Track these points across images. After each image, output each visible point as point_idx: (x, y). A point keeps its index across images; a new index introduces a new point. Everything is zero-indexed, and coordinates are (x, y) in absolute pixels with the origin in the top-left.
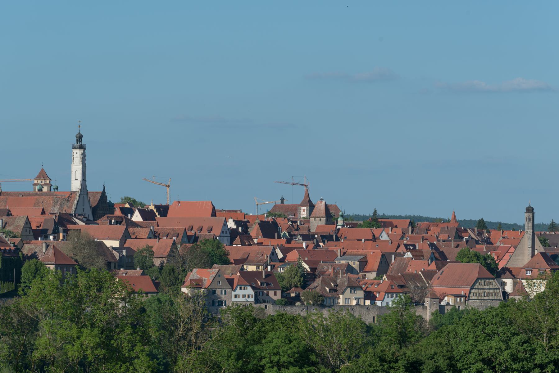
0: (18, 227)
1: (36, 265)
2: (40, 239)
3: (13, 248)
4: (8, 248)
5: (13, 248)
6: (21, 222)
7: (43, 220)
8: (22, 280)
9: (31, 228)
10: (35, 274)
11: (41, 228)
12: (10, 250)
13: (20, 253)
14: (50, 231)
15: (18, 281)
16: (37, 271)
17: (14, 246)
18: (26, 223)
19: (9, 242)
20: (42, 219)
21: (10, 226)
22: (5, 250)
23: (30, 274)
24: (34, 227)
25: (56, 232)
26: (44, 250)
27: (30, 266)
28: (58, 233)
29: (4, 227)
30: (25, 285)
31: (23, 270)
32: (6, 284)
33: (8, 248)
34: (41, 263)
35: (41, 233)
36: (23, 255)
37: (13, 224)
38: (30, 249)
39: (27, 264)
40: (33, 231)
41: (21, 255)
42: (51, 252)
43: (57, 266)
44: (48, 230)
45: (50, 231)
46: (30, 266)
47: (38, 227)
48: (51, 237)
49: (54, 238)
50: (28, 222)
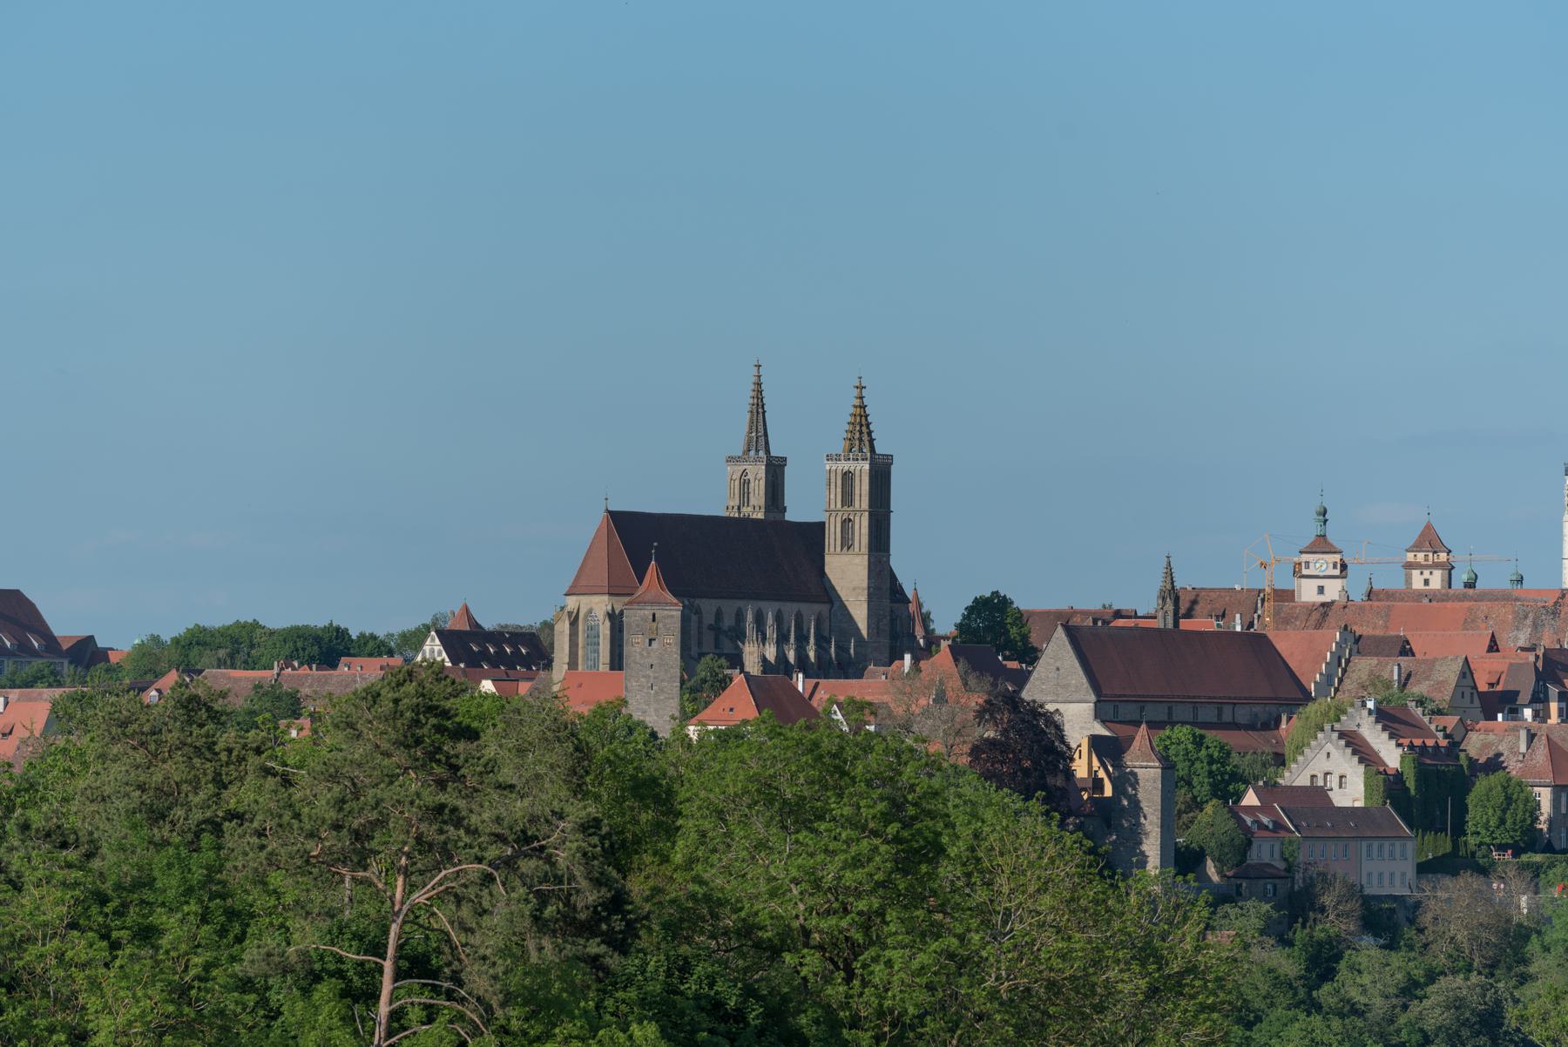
0: (1441, 683)
1: (1505, 788)
2: (1500, 716)
3: (1444, 743)
4: (1430, 743)
5: (1444, 743)
6: (1449, 673)
7: (1504, 668)
8: (1470, 827)
9: (1475, 687)
10: (1504, 811)
11: (1499, 688)
12: (1437, 746)
13: (1462, 755)
14: (1525, 697)
15: (1459, 830)
16: (1509, 804)
17: (1446, 736)
18: (1463, 675)
19: (1433, 727)
20: (1497, 663)
21: (1419, 682)
22: (1424, 746)
23: (1490, 812)
24: (1483, 687)
25: (1539, 699)
26: (1523, 748)
27: (1491, 790)
28: (1546, 701)
29: (1405, 685)
30: (1478, 839)
31: (1471, 799)
32: (1429, 837)
33: (1430, 743)
34: (1520, 784)
35: (1499, 702)
36: (1470, 759)
37: (1427, 678)
38: (1486, 746)
39: (1482, 784)
40: (1481, 694)
41: (1464, 762)
42: (1541, 754)
43: (1558, 790)
44: (1517, 693)
45: (1525, 697)
46: (1491, 790)
47: (1491, 685)
48: (1528, 713)
49: (1536, 715)
50: (1467, 672)
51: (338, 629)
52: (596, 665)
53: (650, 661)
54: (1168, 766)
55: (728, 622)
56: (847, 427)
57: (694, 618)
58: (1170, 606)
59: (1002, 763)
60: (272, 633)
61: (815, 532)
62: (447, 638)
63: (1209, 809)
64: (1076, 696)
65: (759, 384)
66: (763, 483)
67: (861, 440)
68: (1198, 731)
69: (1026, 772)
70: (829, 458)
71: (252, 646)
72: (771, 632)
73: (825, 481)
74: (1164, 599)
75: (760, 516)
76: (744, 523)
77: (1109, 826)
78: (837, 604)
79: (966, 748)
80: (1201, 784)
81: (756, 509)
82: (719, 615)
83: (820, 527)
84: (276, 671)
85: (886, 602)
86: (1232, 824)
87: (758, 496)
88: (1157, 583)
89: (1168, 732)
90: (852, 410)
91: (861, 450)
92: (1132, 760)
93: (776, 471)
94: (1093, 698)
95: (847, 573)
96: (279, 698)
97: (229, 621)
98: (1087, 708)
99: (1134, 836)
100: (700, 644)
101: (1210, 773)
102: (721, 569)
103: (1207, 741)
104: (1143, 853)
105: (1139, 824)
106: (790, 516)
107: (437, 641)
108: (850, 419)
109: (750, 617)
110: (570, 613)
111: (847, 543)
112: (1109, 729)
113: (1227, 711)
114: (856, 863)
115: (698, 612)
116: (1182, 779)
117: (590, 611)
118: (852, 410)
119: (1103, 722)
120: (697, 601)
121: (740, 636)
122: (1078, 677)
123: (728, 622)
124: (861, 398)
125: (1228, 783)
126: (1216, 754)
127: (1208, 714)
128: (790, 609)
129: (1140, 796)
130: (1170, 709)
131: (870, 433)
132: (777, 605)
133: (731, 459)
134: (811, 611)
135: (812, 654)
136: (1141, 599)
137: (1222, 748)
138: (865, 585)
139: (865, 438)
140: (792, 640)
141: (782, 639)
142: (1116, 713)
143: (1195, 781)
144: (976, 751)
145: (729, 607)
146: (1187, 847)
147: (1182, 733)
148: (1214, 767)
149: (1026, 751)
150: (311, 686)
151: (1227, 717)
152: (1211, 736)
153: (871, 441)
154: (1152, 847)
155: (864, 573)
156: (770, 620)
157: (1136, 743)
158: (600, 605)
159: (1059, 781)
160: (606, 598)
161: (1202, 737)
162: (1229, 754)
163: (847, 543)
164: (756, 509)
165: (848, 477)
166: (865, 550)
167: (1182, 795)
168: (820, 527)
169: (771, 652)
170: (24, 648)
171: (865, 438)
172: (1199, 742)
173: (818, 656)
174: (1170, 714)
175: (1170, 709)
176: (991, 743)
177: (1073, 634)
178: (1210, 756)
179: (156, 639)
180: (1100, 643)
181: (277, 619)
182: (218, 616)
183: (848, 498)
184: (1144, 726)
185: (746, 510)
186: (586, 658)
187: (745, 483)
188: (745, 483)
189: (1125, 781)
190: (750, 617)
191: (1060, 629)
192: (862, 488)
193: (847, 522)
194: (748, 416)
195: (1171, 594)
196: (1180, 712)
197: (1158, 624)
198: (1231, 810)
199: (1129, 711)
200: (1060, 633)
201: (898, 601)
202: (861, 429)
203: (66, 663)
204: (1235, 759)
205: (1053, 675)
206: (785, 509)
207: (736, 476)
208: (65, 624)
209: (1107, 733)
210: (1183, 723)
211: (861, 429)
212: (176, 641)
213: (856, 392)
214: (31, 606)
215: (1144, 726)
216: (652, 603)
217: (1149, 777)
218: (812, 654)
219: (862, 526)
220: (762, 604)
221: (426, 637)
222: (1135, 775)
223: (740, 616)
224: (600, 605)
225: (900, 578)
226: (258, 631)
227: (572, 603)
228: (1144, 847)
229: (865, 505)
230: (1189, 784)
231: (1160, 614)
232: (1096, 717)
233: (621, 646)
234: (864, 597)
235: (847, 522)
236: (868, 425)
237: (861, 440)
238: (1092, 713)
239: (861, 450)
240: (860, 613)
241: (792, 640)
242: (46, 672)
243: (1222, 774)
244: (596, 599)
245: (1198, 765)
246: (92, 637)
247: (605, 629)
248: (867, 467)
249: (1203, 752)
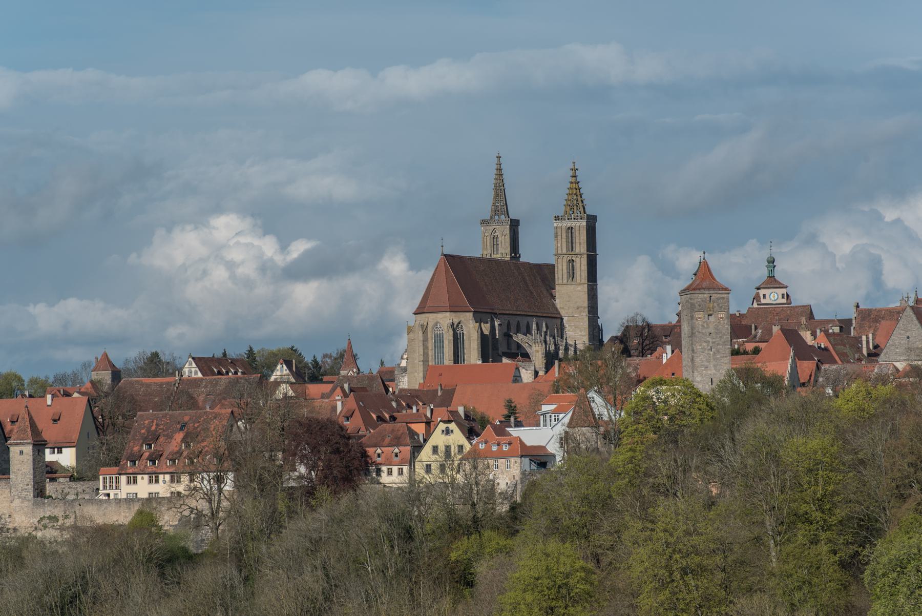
65: (501, 170)
66: (508, 237)
83: (553, 266)
107: (194, 365)
111: (572, 274)
150: (206, 387)
158: (445, 320)
165: (571, 229)
171: (581, 204)
187: (495, 238)
192: (581, 239)
194: (493, 192)
202: (575, 199)
211: (575, 199)
219: (581, 265)
244: (440, 315)
248: (585, 223)
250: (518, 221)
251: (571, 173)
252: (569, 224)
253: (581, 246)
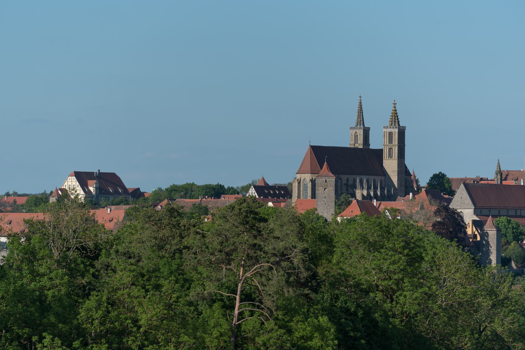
51: (221, 185)
52: (306, 197)
53: (325, 196)
54: (499, 230)
55: (351, 182)
56: (390, 117)
57: (339, 181)
58: (499, 177)
59: (443, 229)
60: (199, 187)
61: (379, 153)
62: (257, 188)
63: (512, 244)
64: (468, 207)
65: (361, 103)
66: (362, 136)
67: (395, 121)
68: (509, 218)
69: (451, 232)
70: (384, 127)
71: (192, 191)
72: (365, 186)
73: (383, 135)
74: (497, 174)
75: (361, 147)
76: (356, 149)
77: (479, 250)
78: (387, 176)
79: (431, 224)
80: (510, 236)
81: (360, 145)
82: (348, 180)
83: (381, 151)
84: (200, 199)
85: (404, 175)
86: (520, 249)
87: (361, 140)
88: (495, 169)
89: (498, 219)
90: (392, 111)
91: (395, 125)
92: (486, 228)
93: (366, 132)
94: (473, 207)
95: (391, 166)
96: (201, 208)
97: (185, 183)
98: (472, 211)
99: (488, 253)
100: (341, 190)
101: (513, 232)
102: (349, 164)
103: (512, 222)
104: (490, 259)
105: (489, 250)
106: (372, 147)
107: (254, 189)
108: (391, 115)
109: (358, 181)
110: (298, 180)
111: (390, 156)
112: (479, 218)
113: (519, 211)
114: (394, 263)
115: (341, 179)
116: (503, 234)
117: (305, 179)
118: (392, 111)
119: (477, 215)
120: (340, 176)
121: (355, 187)
122: (468, 201)
123: (351, 182)
124: (395, 107)
125: (519, 236)
126: (515, 226)
127: (512, 213)
128: (371, 178)
129: (489, 240)
130: (499, 211)
131: (398, 119)
132: (367, 177)
133: (351, 128)
134: (378, 179)
135: (379, 193)
136: (489, 174)
137: (517, 224)
138: (397, 170)
139: (396, 121)
140: (372, 188)
141: (369, 188)
142: (481, 212)
143: (508, 235)
144: (434, 225)
145: (351, 178)
146: (505, 257)
147: (503, 219)
148: (514, 230)
149: (451, 225)
150: (212, 204)
151: (518, 214)
152: (513, 220)
153: (398, 122)
154: (493, 257)
155: (397, 166)
156: (365, 182)
157: (488, 222)
158: (308, 177)
159: (462, 235)
160: (310, 174)
161: (510, 220)
162: (519, 226)
163: (390, 156)
164: (360, 145)
165: (391, 134)
166: (396, 158)
167: (503, 240)
168: (381, 151)
169: (365, 193)
170: (116, 192)
171: (396, 121)
172: (509, 222)
173: (381, 194)
174: (499, 213)
175: (499, 211)
176: (439, 223)
177: (467, 186)
178: (513, 227)
179: (160, 189)
180: (476, 189)
181: (200, 182)
182: (181, 182)
183: (391, 141)
184: (490, 217)
185: (356, 145)
186: (303, 195)
187: (356, 136)
188: (356, 136)
189: (484, 235)
190: (358, 181)
191: (462, 184)
192: (396, 137)
193: (390, 149)
194: (357, 114)
195: (500, 172)
196: (503, 212)
197: (495, 182)
198: (520, 245)
199: (485, 212)
200: (462, 186)
201: (408, 175)
202: (395, 118)
203: (130, 197)
204: (521, 228)
205: (460, 200)
206: (369, 145)
207: (353, 134)
208: (130, 184)
209: (478, 219)
210: (504, 216)
211: (395, 118)
212: (167, 190)
213: (393, 105)
214: (119, 178)
215: (490, 217)
216: (325, 176)
217: (492, 233)
218: (379, 193)
220: (362, 177)
221: (250, 188)
222: (487, 233)
223: (355, 181)
224: (308, 177)
225: (409, 167)
226: (194, 186)
227: (298, 176)
228: (491, 257)
229: (396, 143)
230: (506, 236)
231: (496, 179)
232: (474, 214)
233: (315, 191)
234: (396, 174)
235: (390, 149)
236: (397, 116)
237: (395, 121)
238: (473, 212)
239: (395, 125)
240: (395, 179)
241: (372, 188)
242: (124, 200)
243: (517, 233)
244: (306, 175)
245: (509, 230)
246: (139, 189)
247: (309, 185)
248: (397, 130)
249: (511, 225)
250: (369, 128)
251: (393, 105)
252: (389, 130)
253: (395, 141)
